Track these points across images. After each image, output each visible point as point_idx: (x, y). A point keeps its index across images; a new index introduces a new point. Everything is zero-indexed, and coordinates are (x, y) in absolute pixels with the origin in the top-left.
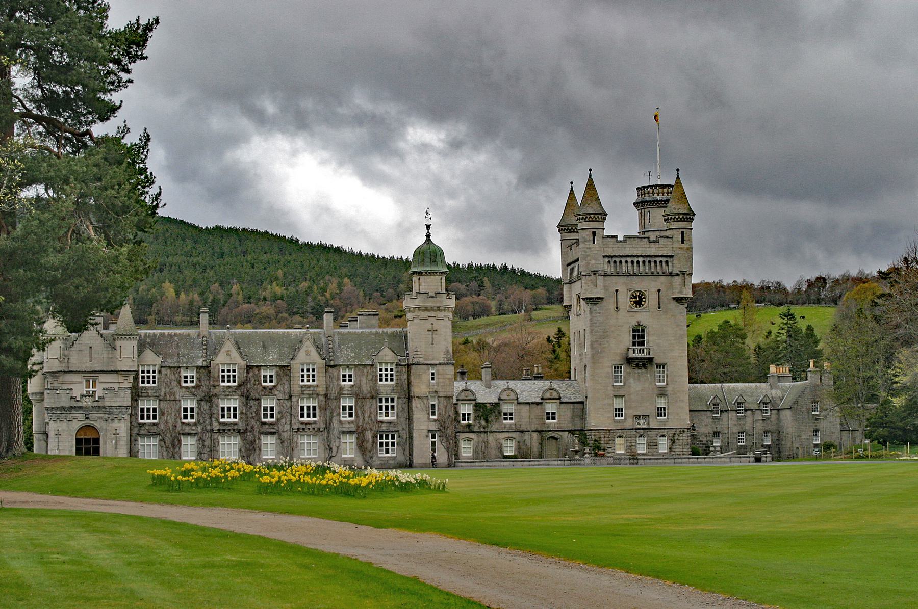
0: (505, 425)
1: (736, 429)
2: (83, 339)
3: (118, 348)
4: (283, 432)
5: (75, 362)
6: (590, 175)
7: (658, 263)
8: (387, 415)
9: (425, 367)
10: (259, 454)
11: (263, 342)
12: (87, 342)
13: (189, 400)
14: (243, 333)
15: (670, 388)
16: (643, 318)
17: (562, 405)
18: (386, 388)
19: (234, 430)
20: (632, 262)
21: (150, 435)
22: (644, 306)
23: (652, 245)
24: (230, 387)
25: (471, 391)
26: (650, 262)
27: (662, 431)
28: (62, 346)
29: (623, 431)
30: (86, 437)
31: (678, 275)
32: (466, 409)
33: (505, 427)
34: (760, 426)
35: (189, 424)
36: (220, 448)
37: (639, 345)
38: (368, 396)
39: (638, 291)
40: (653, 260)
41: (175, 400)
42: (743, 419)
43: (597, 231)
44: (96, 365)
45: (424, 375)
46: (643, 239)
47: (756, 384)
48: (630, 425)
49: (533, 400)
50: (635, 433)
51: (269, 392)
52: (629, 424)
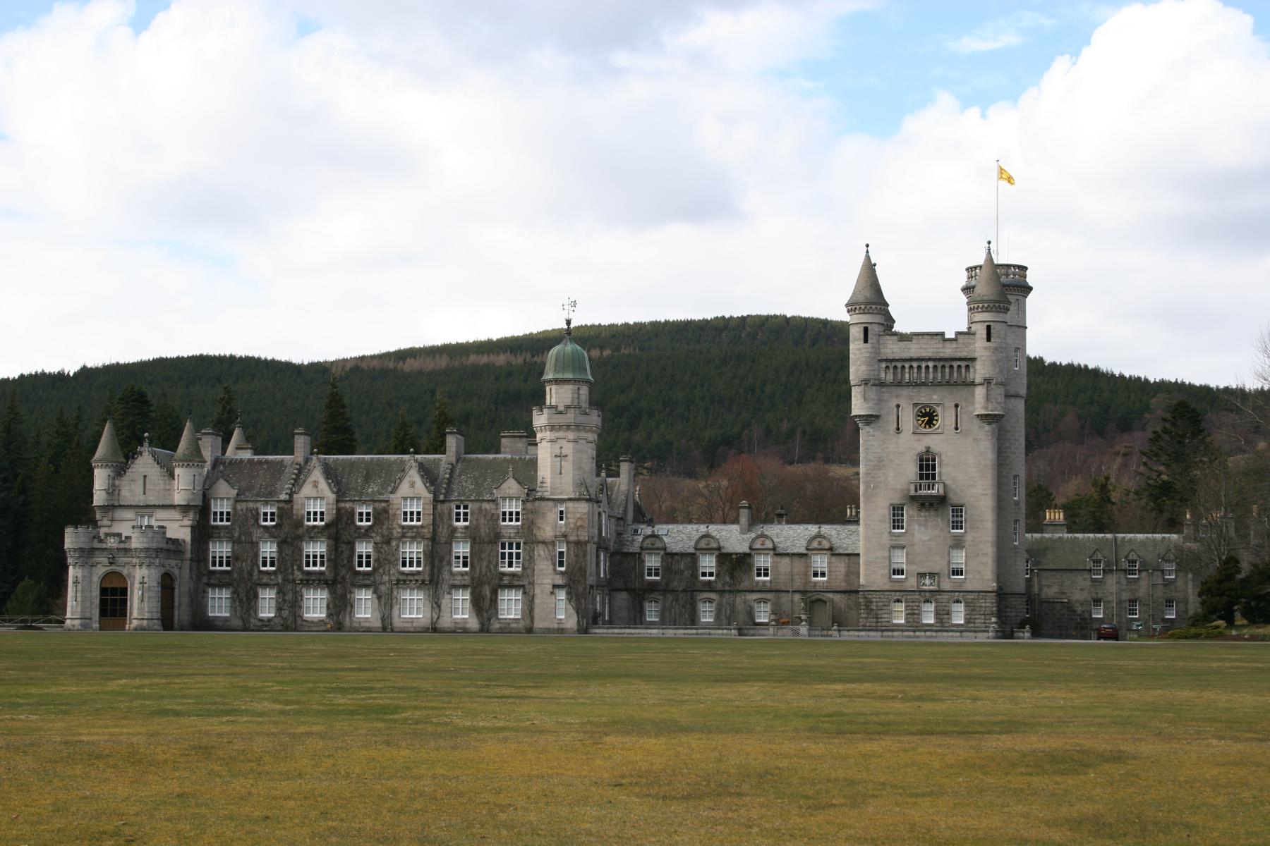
2: (136, 466)
3: (176, 477)
4: (380, 584)
5: (127, 494)
6: (867, 252)
7: (955, 369)
8: (510, 565)
9: (551, 504)
10: (350, 612)
11: (368, 472)
12: (142, 470)
13: (269, 543)
14: (347, 459)
15: (968, 538)
16: (934, 442)
17: (834, 559)
18: (509, 531)
19: (320, 580)
20: (919, 367)
21: (221, 585)
22: (936, 427)
23: (948, 344)
24: (314, 527)
25: (713, 537)
26: (943, 367)
27: (959, 594)
28: (112, 475)
29: (901, 594)
30: (112, 586)
32: (708, 563)
34: (1160, 592)
35: (267, 573)
36: (305, 604)
37: (927, 478)
38: (486, 539)
39: (927, 406)
40: (947, 364)
41: (252, 543)
42: (1135, 582)
43: (870, 327)
44: (151, 498)
45: (549, 514)
46: (935, 337)
47: (1164, 535)
48: (912, 586)
49: (796, 551)
50: (917, 597)
51: (366, 534)
52: (912, 583)
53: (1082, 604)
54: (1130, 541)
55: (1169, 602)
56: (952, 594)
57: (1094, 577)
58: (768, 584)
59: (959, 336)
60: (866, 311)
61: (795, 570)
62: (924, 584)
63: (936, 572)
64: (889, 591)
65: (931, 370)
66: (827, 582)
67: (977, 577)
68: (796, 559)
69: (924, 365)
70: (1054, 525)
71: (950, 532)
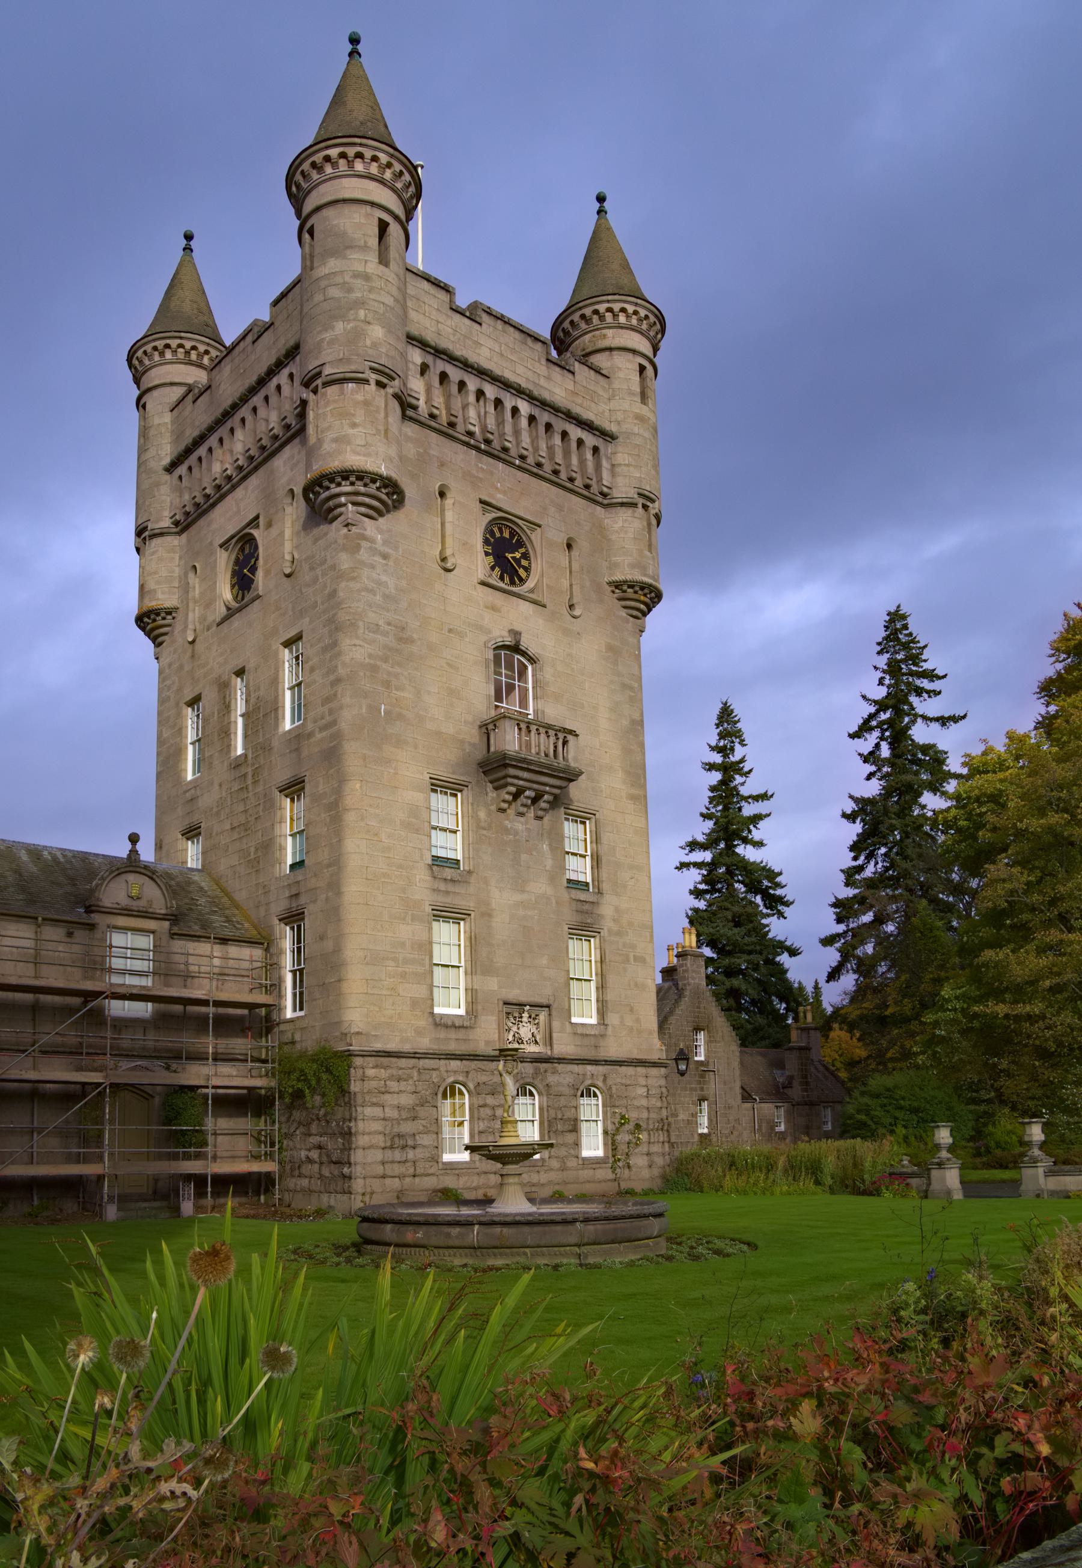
46: (529, 341)
63: (543, 1001)
67: (629, 1021)
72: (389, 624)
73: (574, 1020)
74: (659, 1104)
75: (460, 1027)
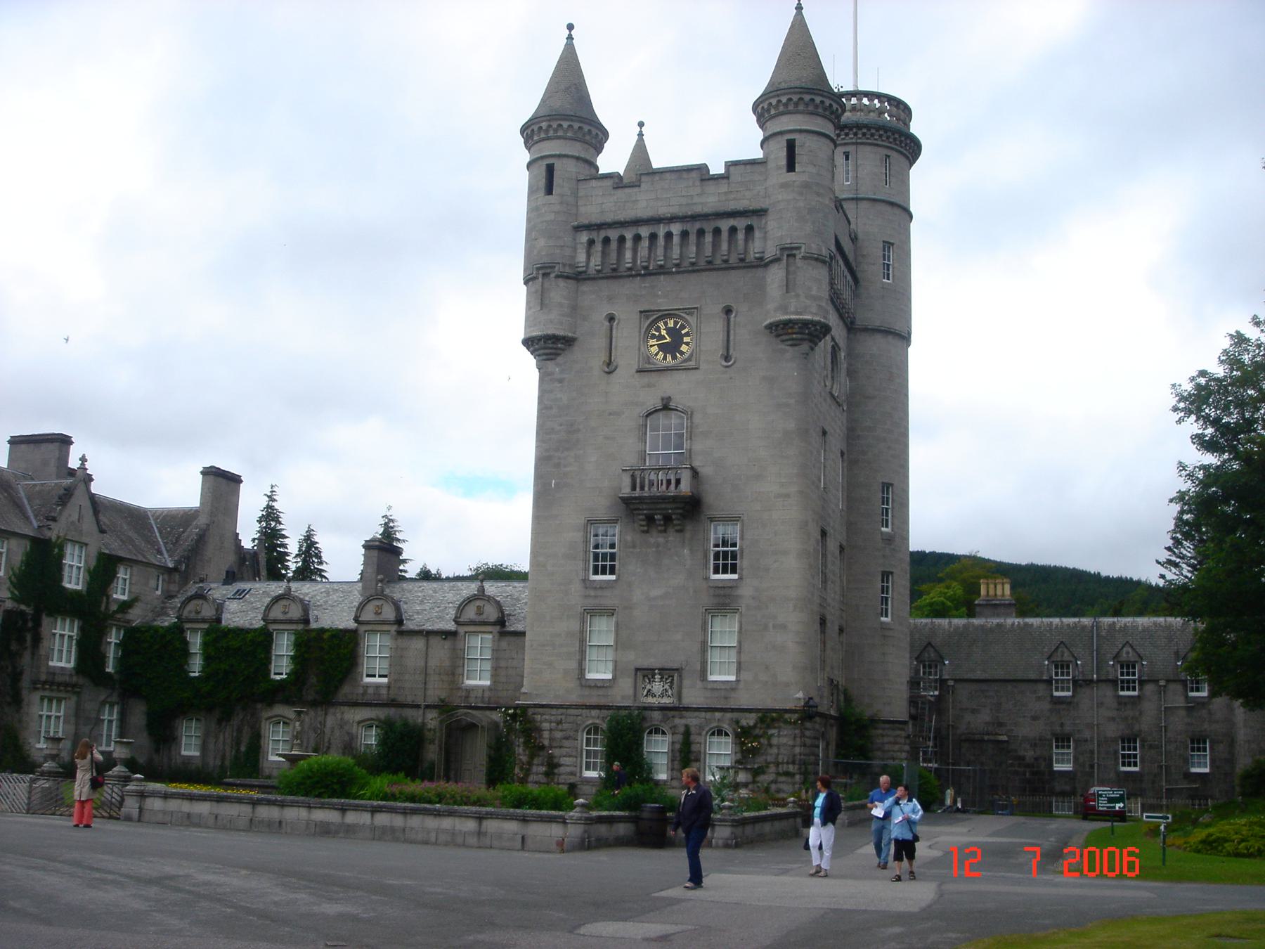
0: (367, 686)
1: (1112, 730)
7: (725, 235)
15: (746, 591)
16: (677, 387)
23: (711, 188)
26: (701, 233)
31: (776, 260)
33: (365, 693)
34: (1178, 722)
40: (709, 227)
43: (558, 165)
46: (685, 175)
48: (623, 697)
53: (1034, 745)
54: (1125, 629)
55: (1198, 741)
56: (709, 715)
57: (1056, 694)
58: (384, 692)
59: (732, 169)
60: (551, 133)
61: (433, 663)
62: (650, 693)
63: (675, 666)
64: (577, 707)
65: (676, 240)
66: (490, 688)
68: (435, 641)
69: (661, 231)
70: (995, 607)
71: (707, 579)
72: (561, 425)
73: (712, 678)
74: (791, 743)
75: (600, 687)
